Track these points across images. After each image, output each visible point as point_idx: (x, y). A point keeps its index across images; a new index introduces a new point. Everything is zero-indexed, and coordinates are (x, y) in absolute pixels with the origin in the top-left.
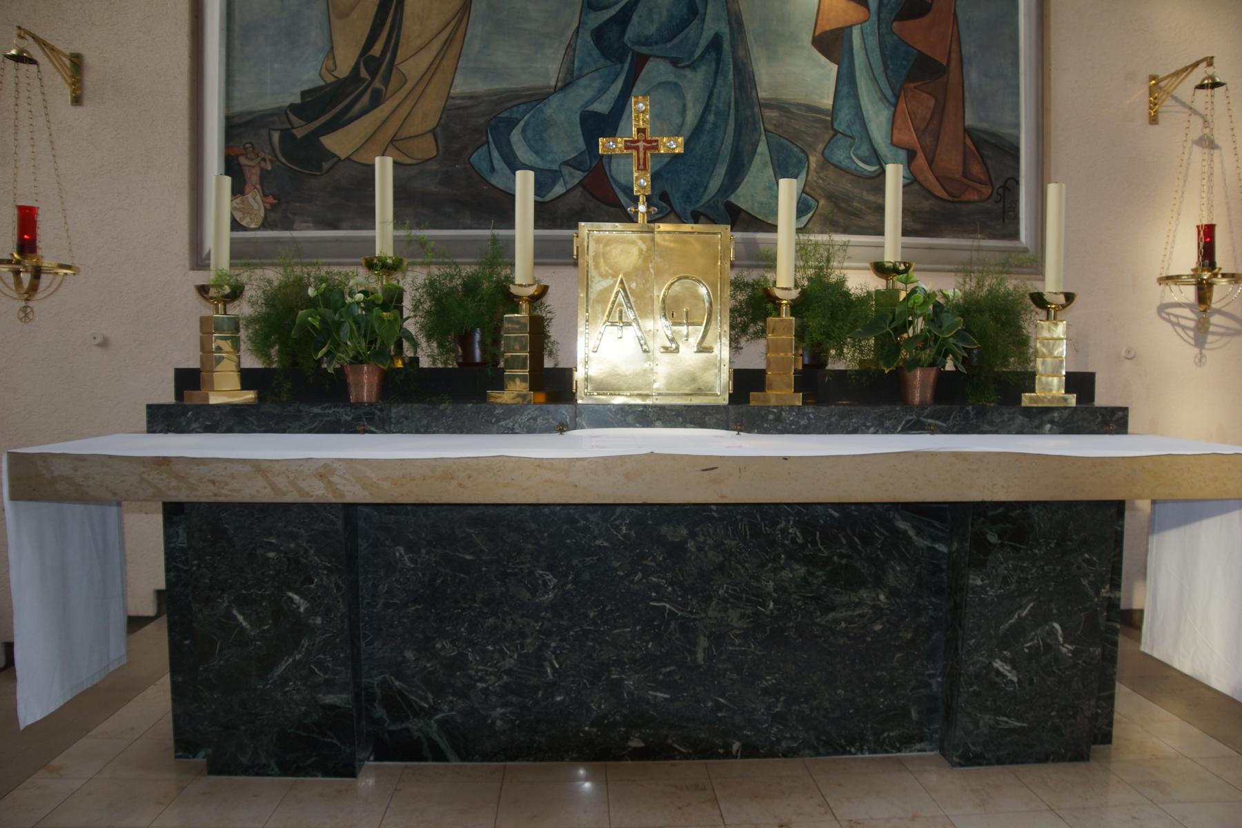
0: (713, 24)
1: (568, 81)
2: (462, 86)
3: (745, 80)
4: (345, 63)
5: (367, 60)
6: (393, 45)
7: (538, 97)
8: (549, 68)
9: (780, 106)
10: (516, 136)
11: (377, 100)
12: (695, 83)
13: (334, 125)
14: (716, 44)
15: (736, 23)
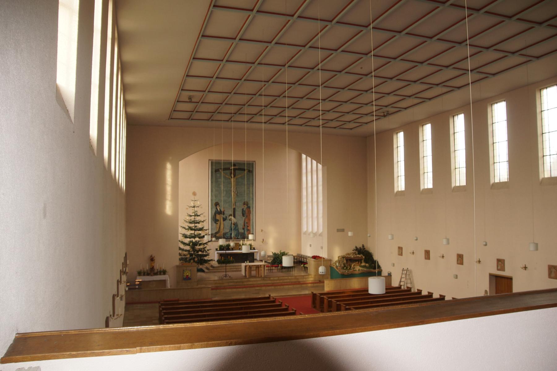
0: (237, 228)
1: (229, 231)
2: (224, 232)
3: (239, 231)
4: (217, 231)
5: (218, 231)
6: (220, 230)
7: (228, 233)
8: (228, 231)
9: (241, 233)
10: (227, 235)
11: (219, 233)
12: (236, 231)
13: (217, 234)
14: (237, 229)
15: (238, 228)
